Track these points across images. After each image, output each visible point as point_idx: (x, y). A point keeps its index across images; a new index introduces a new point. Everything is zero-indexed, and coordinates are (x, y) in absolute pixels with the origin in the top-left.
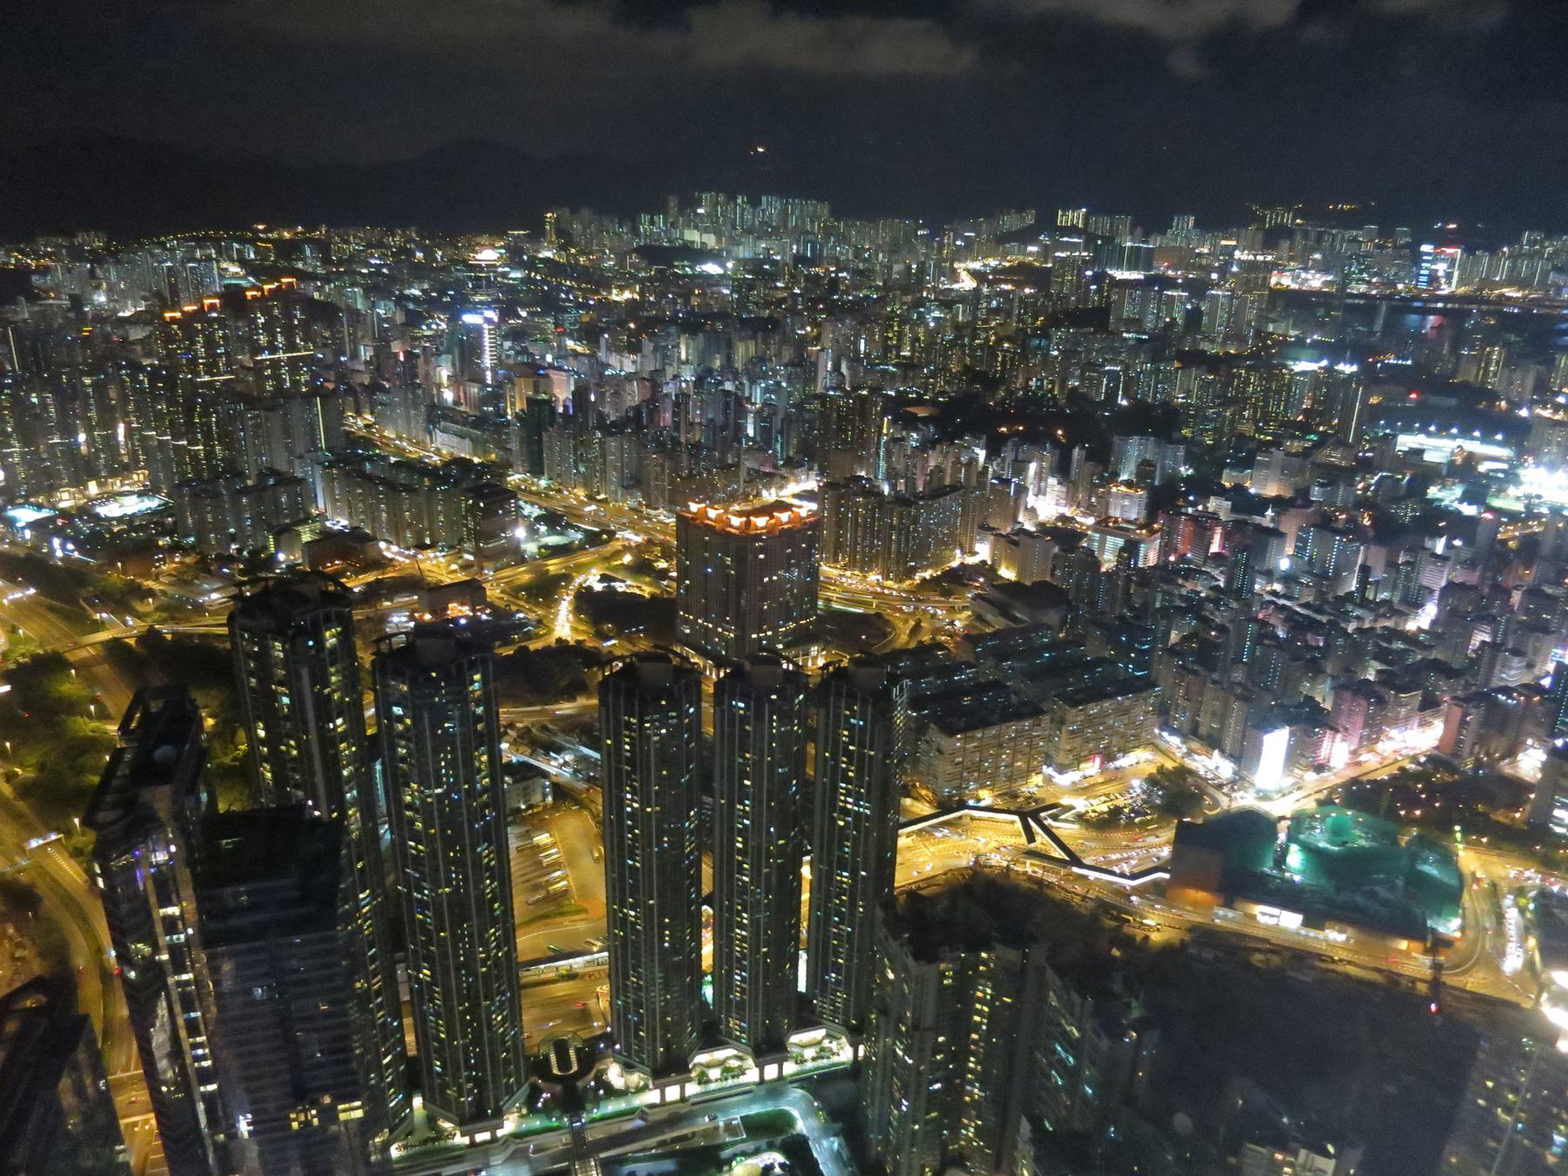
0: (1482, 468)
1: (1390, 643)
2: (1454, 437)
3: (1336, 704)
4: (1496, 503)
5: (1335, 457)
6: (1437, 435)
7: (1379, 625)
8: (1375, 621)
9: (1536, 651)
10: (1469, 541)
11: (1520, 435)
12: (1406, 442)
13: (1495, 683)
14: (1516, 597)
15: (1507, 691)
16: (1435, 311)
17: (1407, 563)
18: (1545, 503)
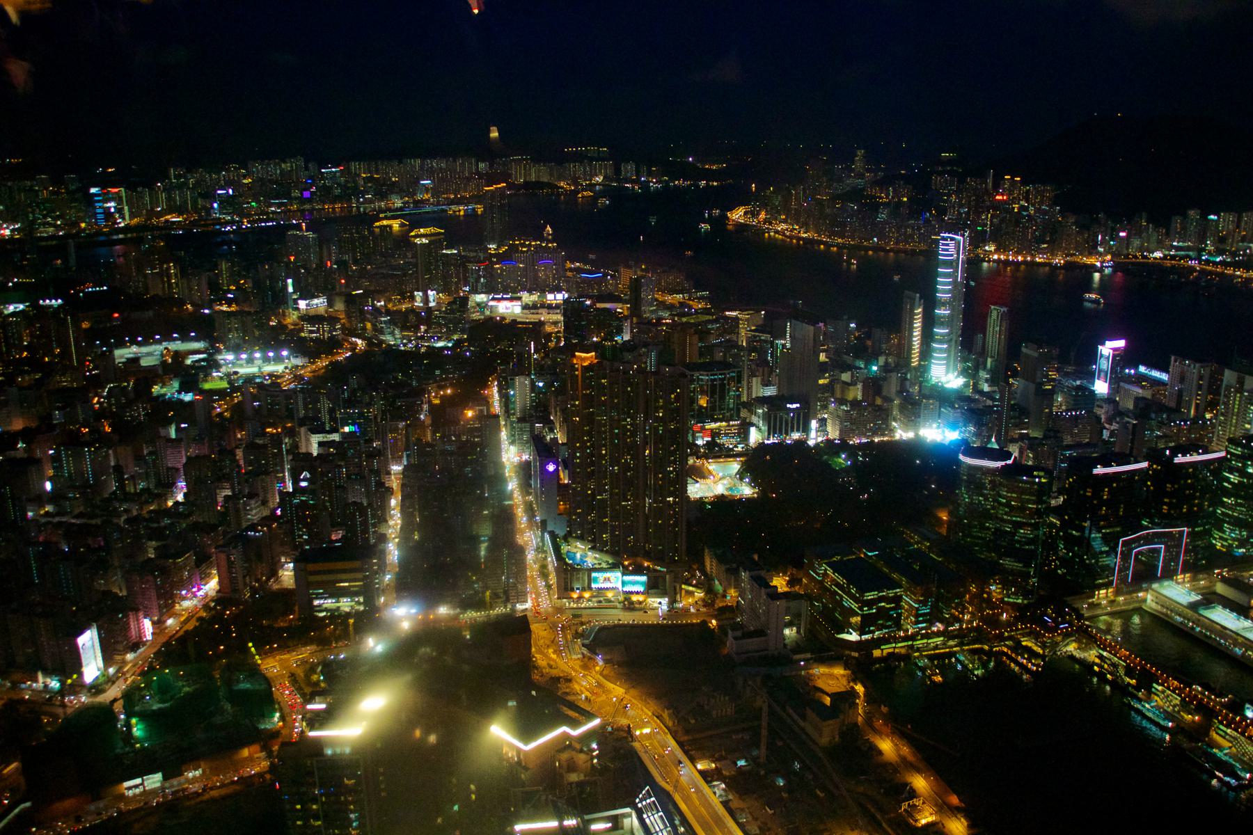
0: (188, 362)
1: (159, 522)
2: (159, 342)
3: (129, 589)
4: (207, 386)
5: (65, 382)
6: (145, 343)
7: (144, 512)
8: (141, 509)
9: (265, 491)
10: (192, 423)
11: (209, 330)
12: (123, 354)
13: (244, 525)
14: (239, 454)
15: (253, 527)
16: (120, 242)
17: (150, 453)
18: (241, 377)
